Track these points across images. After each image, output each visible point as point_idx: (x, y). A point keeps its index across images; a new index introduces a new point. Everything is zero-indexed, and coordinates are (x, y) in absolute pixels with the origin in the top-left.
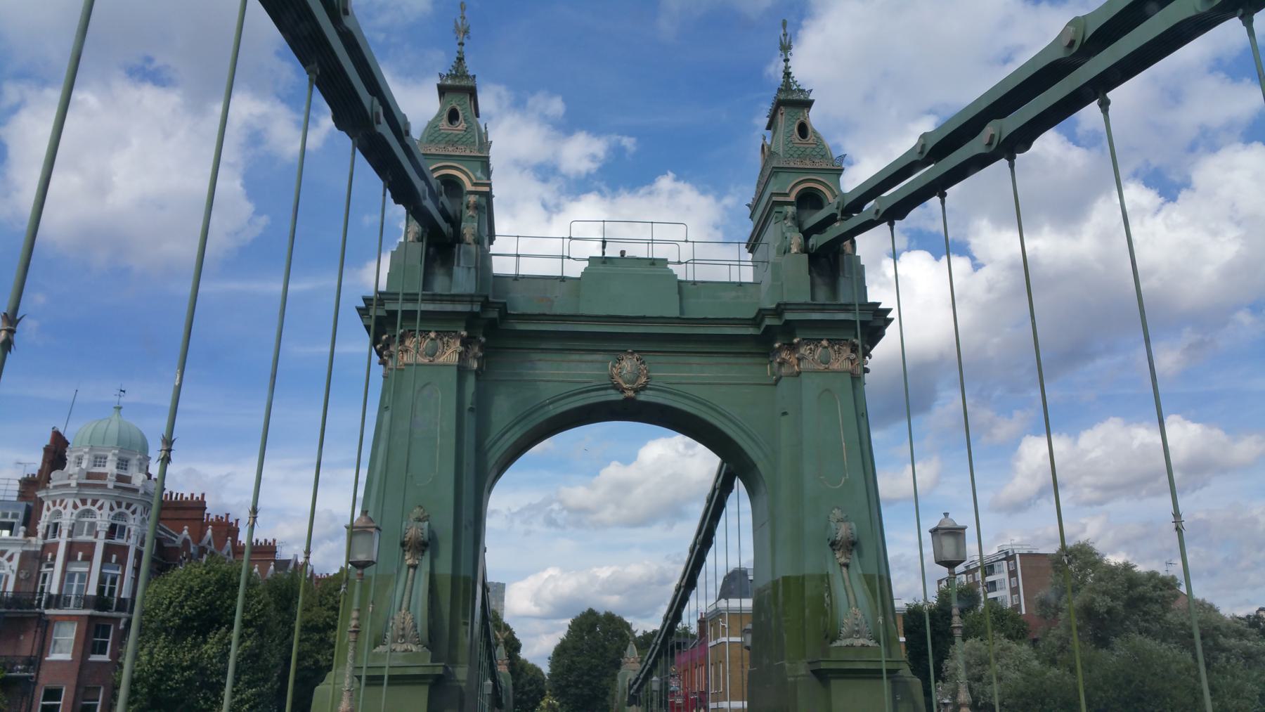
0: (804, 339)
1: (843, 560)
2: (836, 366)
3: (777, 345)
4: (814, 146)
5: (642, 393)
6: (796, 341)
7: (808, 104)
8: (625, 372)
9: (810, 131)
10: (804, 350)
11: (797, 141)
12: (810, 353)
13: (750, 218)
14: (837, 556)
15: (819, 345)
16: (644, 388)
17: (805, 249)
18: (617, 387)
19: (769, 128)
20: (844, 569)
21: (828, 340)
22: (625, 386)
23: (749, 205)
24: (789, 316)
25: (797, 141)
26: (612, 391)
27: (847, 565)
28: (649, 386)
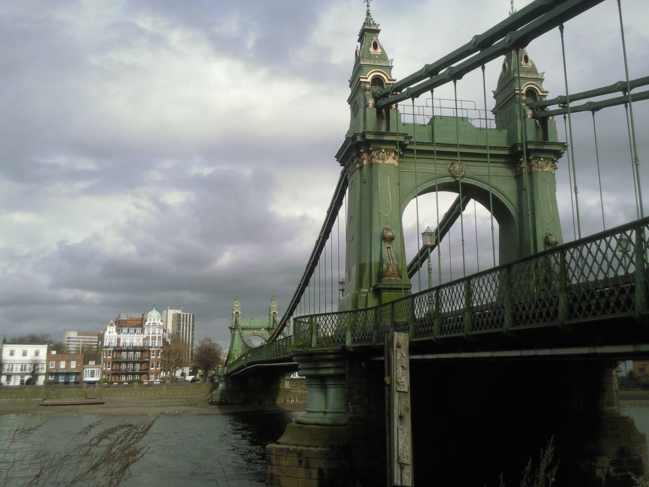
3: (362, 151)
6: (371, 149)
7: (378, 31)
17: (375, 106)
20: (389, 249)
23: (349, 81)
24: (369, 137)
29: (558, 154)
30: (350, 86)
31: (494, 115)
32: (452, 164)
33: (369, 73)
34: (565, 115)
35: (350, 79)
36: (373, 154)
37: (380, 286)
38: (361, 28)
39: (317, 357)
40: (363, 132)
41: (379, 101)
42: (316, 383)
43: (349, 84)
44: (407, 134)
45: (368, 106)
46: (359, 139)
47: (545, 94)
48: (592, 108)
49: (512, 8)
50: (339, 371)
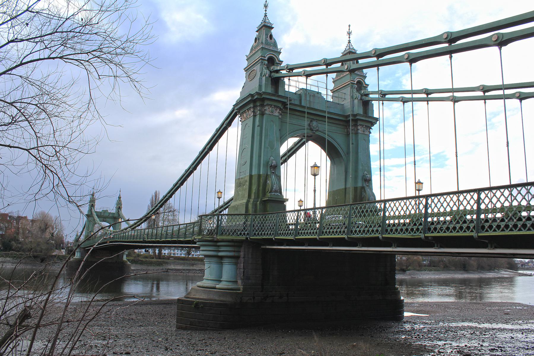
0: (267, 104)
9: (273, 39)
10: (266, 108)
17: (270, 76)
19: (257, 31)
21: (274, 105)
23: (247, 56)
29: (373, 124)
31: (332, 93)
32: (311, 121)
34: (383, 102)
39: (219, 244)
41: (273, 74)
42: (208, 261)
47: (366, 86)
48: (403, 101)
49: (349, 29)
50: (236, 254)
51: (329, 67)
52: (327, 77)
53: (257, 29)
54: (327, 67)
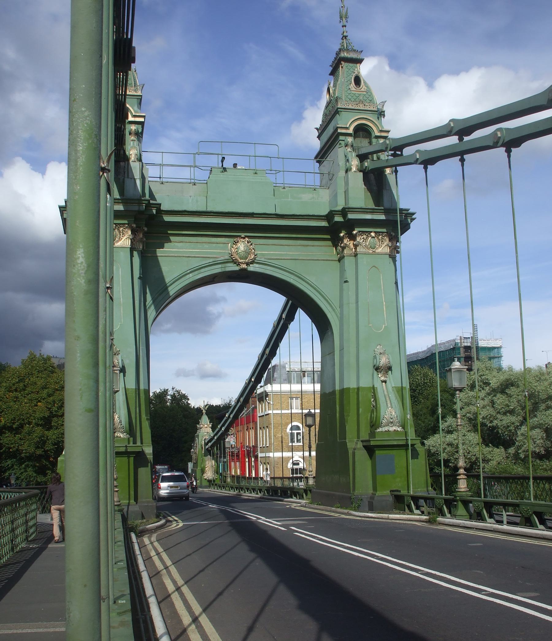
0: (359, 232)
1: (383, 378)
2: (379, 250)
4: (365, 93)
5: (251, 265)
8: (240, 251)
9: (362, 82)
11: (354, 89)
12: (364, 241)
13: (317, 137)
14: (380, 376)
15: (369, 235)
16: (253, 262)
17: (361, 170)
18: (235, 262)
21: (375, 232)
22: (240, 261)
23: (317, 129)
24: (351, 216)
25: (354, 89)
26: (231, 264)
27: (385, 382)
28: (256, 261)
30: (319, 137)
33: (353, 120)
35: (318, 126)
36: (358, 239)
37: (372, 443)
38: (335, 56)
40: (344, 209)
43: (317, 134)
44: (408, 210)
45: (351, 169)
46: (338, 219)
51: (466, 139)
52: (463, 165)
53: (331, 69)
54: (461, 139)
